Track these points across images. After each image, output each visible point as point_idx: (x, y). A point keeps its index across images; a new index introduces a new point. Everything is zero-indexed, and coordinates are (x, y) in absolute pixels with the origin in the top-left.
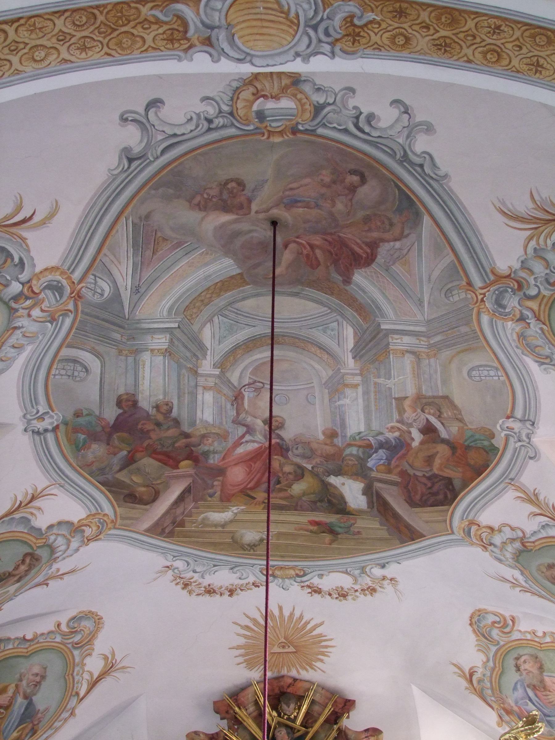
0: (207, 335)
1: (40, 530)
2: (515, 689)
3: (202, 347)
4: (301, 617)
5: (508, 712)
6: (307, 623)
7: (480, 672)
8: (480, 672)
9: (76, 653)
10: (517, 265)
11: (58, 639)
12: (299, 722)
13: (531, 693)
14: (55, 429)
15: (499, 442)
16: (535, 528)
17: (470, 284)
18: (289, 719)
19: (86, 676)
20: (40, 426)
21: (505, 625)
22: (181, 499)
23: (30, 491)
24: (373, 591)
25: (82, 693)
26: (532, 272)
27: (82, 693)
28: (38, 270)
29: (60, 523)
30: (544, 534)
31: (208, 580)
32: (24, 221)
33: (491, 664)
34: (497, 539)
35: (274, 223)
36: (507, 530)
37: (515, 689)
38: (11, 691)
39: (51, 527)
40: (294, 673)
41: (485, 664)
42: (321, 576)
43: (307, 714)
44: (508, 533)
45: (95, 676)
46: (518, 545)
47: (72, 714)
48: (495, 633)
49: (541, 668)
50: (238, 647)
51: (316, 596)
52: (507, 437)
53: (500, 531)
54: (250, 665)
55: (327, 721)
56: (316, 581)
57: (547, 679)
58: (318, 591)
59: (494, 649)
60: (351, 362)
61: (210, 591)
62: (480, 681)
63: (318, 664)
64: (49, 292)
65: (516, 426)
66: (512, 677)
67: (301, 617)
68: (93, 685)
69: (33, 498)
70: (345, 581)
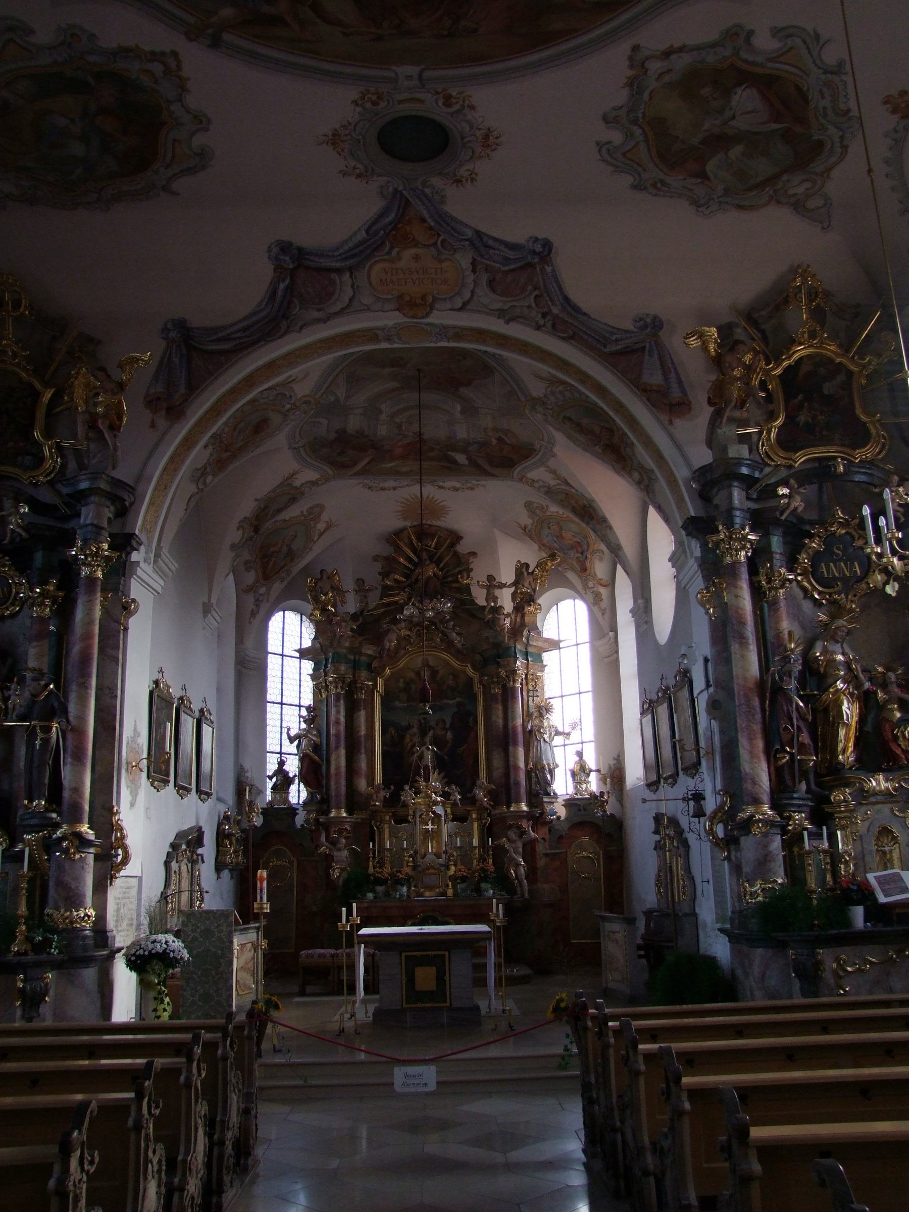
0: (383, 407)
1: (296, 487)
2: (547, 536)
3: (381, 412)
4: (433, 498)
5: (544, 545)
6: (436, 501)
7: (529, 528)
8: (529, 528)
9: (312, 523)
10: (542, 396)
11: (303, 518)
12: (432, 547)
13: (555, 539)
14: (303, 446)
15: (537, 446)
16: (555, 483)
17: (519, 399)
18: (427, 546)
19: (317, 532)
20: (296, 446)
21: (543, 508)
22: (369, 463)
23: (291, 472)
24: (472, 489)
25: (315, 540)
26: (549, 400)
27: (315, 540)
28: (299, 397)
29: (306, 483)
30: (558, 487)
31: (381, 485)
32: (292, 381)
33: (535, 524)
34: (536, 485)
35: (419, 370)
36: (541, 482)
37: (547, 536)
38: (279, 545)
39: (303, 484)
40: (429, 522)
41: (532, 525)
42: (444, 482)
43: (437, 543)
44: (541, 483)
45: (322, 531)
46: (546, 489)
47: (311, 549)
48: (538, 511)
49: (561, 529)
50: (398, 512)
51: (443, 490)
52: (540, 447)
53: (537, 482)
54: (405, 519)
55: (448, 547)
56: (441, 484)
57: (564, 534)
58: (443, 488)
59: (536, 518)
60: (458, 415)
61: (383, 489)
62: (529, 531)
63: (443, 518)
64: (304, 405)
65: (545, 444)
66: (546, 531)
67: (433, 498)
68: (320, 535)
69: (293, 474)
70: (458, 485)
